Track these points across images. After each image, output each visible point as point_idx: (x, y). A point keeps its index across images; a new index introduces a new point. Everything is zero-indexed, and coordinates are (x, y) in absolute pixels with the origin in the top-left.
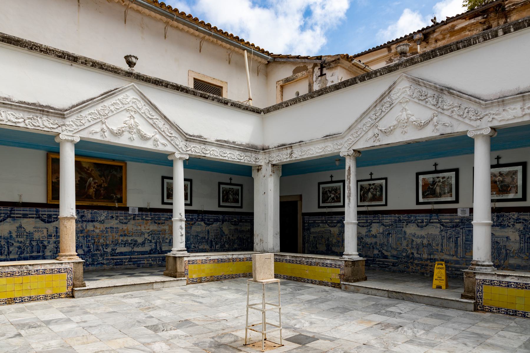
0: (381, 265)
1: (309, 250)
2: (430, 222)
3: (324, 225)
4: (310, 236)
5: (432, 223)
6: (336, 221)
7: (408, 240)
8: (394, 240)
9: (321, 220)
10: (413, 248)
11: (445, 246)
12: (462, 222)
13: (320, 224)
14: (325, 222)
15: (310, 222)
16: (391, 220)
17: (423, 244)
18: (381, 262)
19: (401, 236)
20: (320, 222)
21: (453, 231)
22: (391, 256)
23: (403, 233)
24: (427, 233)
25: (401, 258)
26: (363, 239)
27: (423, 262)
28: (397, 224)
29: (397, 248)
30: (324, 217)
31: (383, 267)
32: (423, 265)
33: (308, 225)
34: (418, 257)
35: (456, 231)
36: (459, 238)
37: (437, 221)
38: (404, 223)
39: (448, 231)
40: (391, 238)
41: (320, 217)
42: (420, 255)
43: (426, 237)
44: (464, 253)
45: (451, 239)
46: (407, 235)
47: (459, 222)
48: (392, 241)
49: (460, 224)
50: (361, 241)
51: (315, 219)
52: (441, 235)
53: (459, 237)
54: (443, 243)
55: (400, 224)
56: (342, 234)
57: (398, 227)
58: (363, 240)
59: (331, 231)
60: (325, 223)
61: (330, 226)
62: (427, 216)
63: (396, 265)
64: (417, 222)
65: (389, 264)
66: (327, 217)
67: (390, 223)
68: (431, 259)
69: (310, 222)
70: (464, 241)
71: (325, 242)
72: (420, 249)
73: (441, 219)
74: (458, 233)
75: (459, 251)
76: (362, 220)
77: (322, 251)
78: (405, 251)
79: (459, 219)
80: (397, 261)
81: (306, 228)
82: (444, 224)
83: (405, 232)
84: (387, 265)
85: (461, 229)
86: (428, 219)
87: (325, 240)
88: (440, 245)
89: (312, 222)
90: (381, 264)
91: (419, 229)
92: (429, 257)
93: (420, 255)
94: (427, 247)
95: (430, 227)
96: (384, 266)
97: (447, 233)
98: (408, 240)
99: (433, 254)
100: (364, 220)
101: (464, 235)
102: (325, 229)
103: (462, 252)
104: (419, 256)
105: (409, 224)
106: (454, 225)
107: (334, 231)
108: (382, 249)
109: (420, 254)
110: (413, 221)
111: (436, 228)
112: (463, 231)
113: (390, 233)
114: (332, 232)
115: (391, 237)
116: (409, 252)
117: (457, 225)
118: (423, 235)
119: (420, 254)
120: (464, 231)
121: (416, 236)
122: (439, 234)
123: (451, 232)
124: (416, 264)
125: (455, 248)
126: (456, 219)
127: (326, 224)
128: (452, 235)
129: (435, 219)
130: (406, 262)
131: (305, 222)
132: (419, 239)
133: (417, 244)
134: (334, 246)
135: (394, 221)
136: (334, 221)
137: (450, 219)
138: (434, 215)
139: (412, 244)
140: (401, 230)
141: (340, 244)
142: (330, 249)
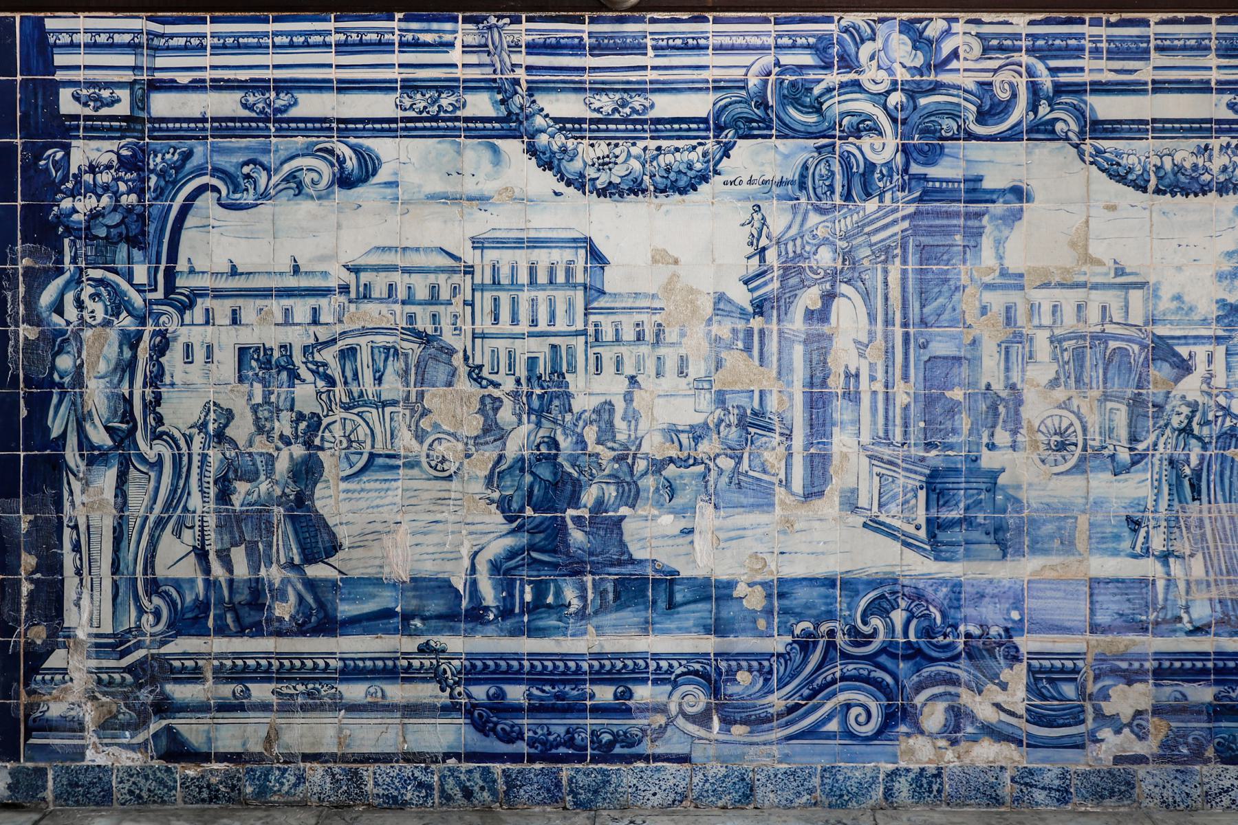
1: (154, 586)
3: (474, 153)
4: (162, 345)
6: (700, 105)
9: (410, 87)
13: (382, 147)
14: (481, 105)
15: (161, 104)
20: (382, 105)
26: (1184, 367)
30: (462, 32)
33: (133, 163)
41: (395, 26)
50: (1153, 392)
51: (266, 66)
56: (810, 297)
58: (1191, 387)
59: (596, 256)
60: (478, 129)
61: (579, 183)
66: (525, 30)
69: (161, 104)
71: (492, 431)
76: (1159, 87)
77: (418, 584)
81: (85, 204)
87: (489, 406)
89: (228, 104)
100: (1204, 88)
102: (483, 223)
107: (660, 257)
114: (612, 280)
127: (512, 148)
131: (67, 104)
134: (672, 490)
136: (666, 106)
141: (772, 456)
142: (577, 536)
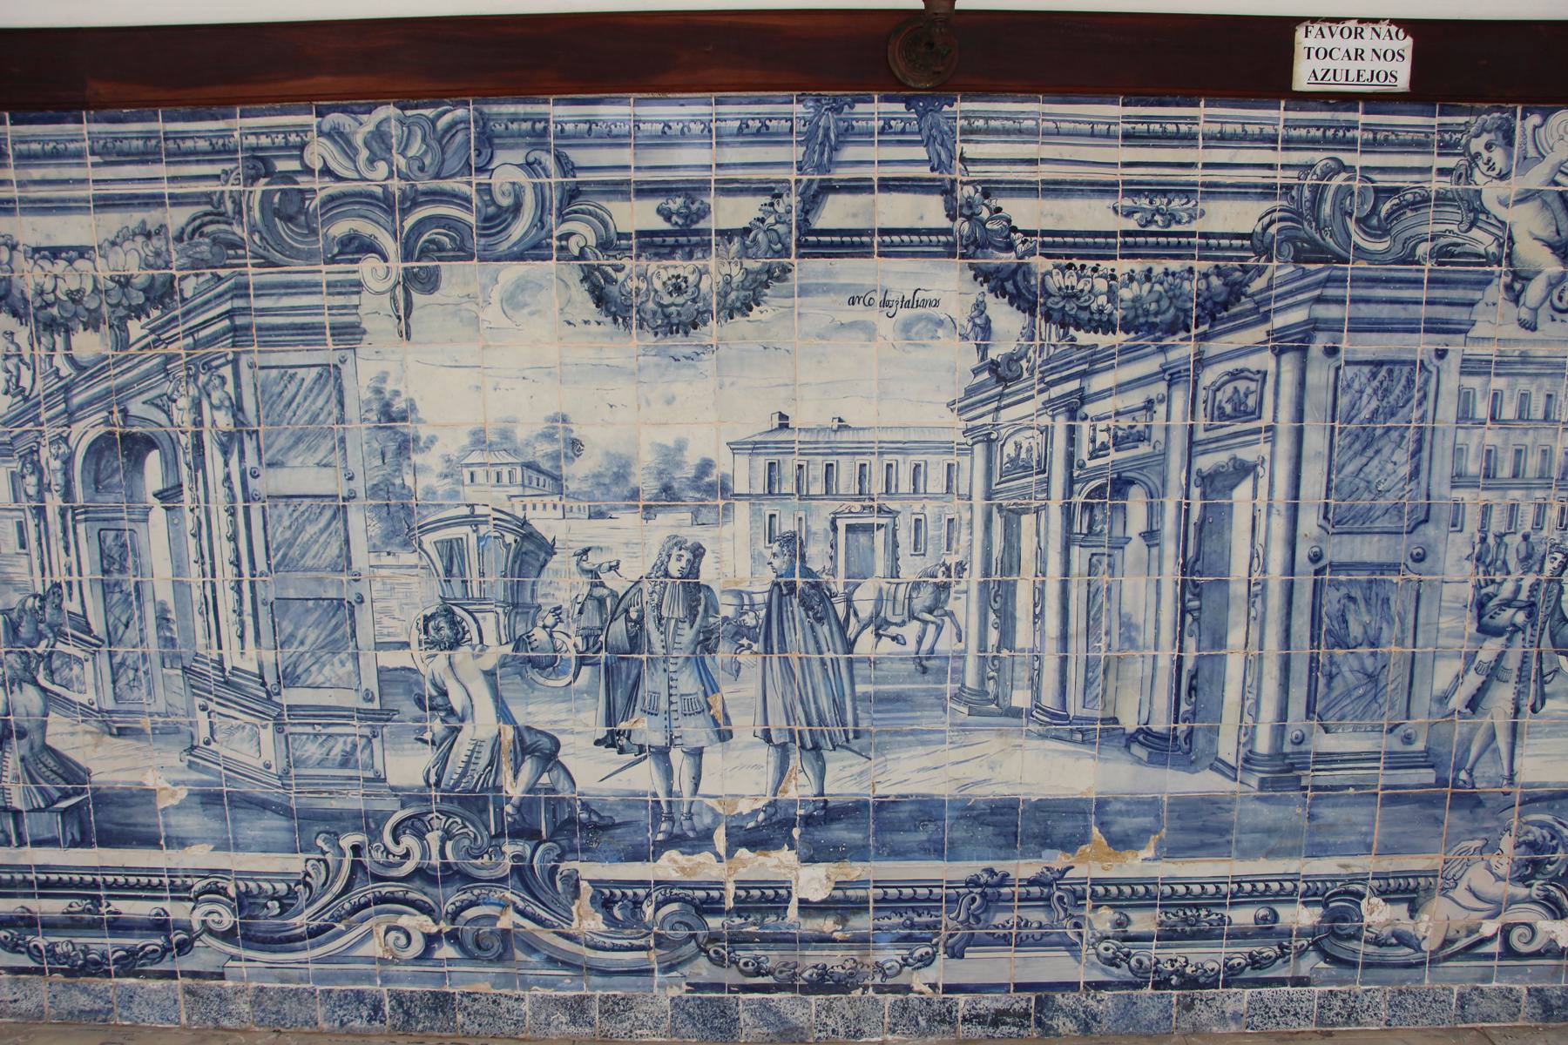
0: (62, 944)
2: (805, 228)
5: (849, 243)
7: (452, 553)
8: (224, 551)
10: (547, 665)
11: (1038, 617)
12: (1308, 253)
16: (134, 218)
17: (694, 592)
18: (47, 888)
19: (326, 482)
21: (1172, 376)
22: (209, 799)
23: (359, 431)
24: (757, 423)
25: (369, 823)
27: (706, 866)
28: (254, 275)
29: (288, 678)
31: (95, 967)
32: (711, 907)
34: (632, 800)
35: (1209, 376)
36: (1243, 491)
37: (930, 211)
38: (368, 268)
39: (1098, 383)
40: (158, 514)
42: (668, 773)
43: (745, 474)
44: (1298, 694)
45: (1136, 503)
46: (430, 460)
47: (1259, 244)
48: (179, 567)
49: (1280, 270)
52: (989, 442)
53: (1244, 470)
54: (1011, 563)
55: (298, 272)
57: (273, 336)
62: (763, 135)
63: (301, 921)
64: (583, 233)
65: (178, 911)
67: (129, 261)
68: (827, 814)
70: (1309, 522)
72: (653, 683)
73: (989, 189)
74: (1241, 411)
75: (1234, 667)
78: (409, 708)
79: (1268, 192)
80: (296, 864)
82: (1040, 264)
83: (390, 415)
84: (160, 925)
85: (1294, 343)
86: (772, 191)
88: (965, 605)
90: (51, 926)
91: (629, 347)
92: (800, 788)
93: (668, 773)
94: (769, 636)
95: (821, 311)
96: (106, 945)
97: (1074, 407)
98: (452, 553)
99: (852, 741)
101: (1315, 441)
103: (1270, 687)
104: (644, 778)
105: (457, 277)
106: (1191, 287)
108: (29, 698)
109: (662, 754)
110: (519, 229)
111: (907, 327)
112: (1302, 384)
113: (150, 443)
115: (170, 495)
116: (483, 724)
117: (1236, 291)
118: (692, 458)
119: (662, 754)
120: (1319, 376)
121: (577, 472)
122: (952, 427)
123: (1136, 398)
124: (605, 904)
125: (1180, 638)
126: (1214, 191)
128: (1141, 438)
129: (887, 185)
130: (452, 875)
132: (629, 520)
133: (606, 605)
135: (196, 230)
137: (1134, 189)
138: (874, 110)
139: (517, 605)
140: (331, 375)
